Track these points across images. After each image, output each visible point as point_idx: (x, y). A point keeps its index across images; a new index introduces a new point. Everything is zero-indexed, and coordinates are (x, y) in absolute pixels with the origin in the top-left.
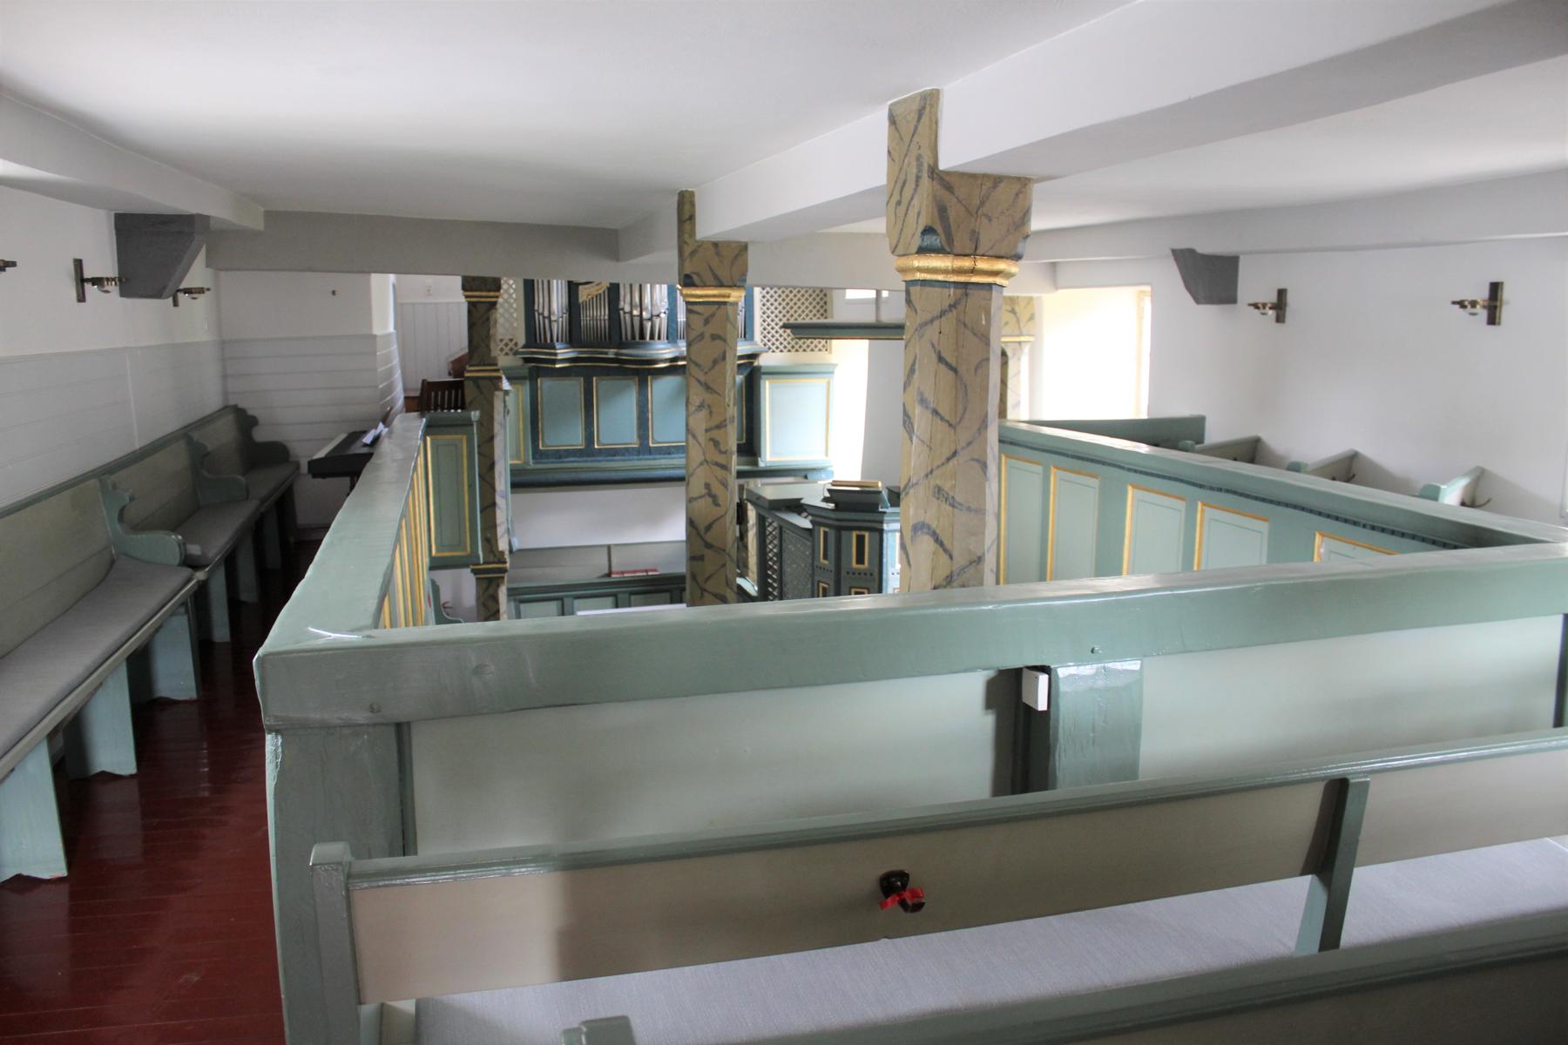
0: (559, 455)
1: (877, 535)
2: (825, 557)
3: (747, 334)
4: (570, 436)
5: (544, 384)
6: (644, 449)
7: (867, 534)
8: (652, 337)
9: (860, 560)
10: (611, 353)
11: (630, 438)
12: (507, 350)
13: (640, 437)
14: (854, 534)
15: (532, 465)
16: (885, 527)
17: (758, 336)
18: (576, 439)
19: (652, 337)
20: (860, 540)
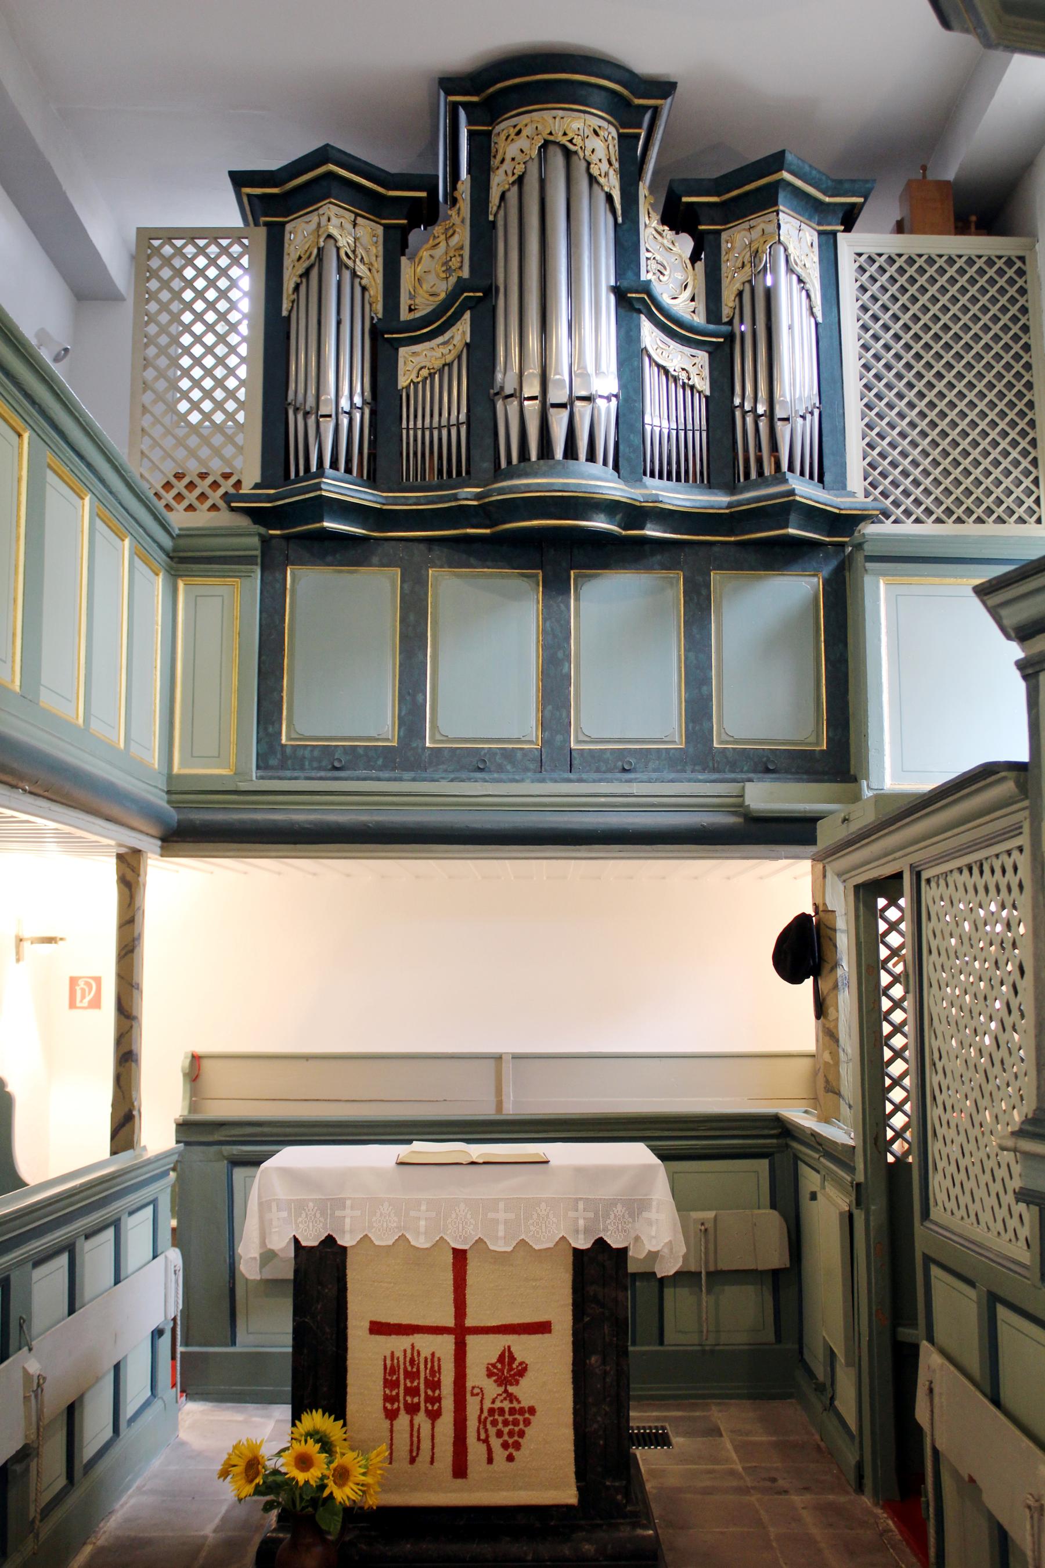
0: (336, 760)
4: (346, 702)
5: (305, 582)
6: (555, 755)
8: (570, 452)
10: (468, 494)
11: (520, 723)
12: (215, 497)
13: (544, 725)
15: (254, 780)
17: (855, 482)
18: (377, 721)
19: (570, 452)
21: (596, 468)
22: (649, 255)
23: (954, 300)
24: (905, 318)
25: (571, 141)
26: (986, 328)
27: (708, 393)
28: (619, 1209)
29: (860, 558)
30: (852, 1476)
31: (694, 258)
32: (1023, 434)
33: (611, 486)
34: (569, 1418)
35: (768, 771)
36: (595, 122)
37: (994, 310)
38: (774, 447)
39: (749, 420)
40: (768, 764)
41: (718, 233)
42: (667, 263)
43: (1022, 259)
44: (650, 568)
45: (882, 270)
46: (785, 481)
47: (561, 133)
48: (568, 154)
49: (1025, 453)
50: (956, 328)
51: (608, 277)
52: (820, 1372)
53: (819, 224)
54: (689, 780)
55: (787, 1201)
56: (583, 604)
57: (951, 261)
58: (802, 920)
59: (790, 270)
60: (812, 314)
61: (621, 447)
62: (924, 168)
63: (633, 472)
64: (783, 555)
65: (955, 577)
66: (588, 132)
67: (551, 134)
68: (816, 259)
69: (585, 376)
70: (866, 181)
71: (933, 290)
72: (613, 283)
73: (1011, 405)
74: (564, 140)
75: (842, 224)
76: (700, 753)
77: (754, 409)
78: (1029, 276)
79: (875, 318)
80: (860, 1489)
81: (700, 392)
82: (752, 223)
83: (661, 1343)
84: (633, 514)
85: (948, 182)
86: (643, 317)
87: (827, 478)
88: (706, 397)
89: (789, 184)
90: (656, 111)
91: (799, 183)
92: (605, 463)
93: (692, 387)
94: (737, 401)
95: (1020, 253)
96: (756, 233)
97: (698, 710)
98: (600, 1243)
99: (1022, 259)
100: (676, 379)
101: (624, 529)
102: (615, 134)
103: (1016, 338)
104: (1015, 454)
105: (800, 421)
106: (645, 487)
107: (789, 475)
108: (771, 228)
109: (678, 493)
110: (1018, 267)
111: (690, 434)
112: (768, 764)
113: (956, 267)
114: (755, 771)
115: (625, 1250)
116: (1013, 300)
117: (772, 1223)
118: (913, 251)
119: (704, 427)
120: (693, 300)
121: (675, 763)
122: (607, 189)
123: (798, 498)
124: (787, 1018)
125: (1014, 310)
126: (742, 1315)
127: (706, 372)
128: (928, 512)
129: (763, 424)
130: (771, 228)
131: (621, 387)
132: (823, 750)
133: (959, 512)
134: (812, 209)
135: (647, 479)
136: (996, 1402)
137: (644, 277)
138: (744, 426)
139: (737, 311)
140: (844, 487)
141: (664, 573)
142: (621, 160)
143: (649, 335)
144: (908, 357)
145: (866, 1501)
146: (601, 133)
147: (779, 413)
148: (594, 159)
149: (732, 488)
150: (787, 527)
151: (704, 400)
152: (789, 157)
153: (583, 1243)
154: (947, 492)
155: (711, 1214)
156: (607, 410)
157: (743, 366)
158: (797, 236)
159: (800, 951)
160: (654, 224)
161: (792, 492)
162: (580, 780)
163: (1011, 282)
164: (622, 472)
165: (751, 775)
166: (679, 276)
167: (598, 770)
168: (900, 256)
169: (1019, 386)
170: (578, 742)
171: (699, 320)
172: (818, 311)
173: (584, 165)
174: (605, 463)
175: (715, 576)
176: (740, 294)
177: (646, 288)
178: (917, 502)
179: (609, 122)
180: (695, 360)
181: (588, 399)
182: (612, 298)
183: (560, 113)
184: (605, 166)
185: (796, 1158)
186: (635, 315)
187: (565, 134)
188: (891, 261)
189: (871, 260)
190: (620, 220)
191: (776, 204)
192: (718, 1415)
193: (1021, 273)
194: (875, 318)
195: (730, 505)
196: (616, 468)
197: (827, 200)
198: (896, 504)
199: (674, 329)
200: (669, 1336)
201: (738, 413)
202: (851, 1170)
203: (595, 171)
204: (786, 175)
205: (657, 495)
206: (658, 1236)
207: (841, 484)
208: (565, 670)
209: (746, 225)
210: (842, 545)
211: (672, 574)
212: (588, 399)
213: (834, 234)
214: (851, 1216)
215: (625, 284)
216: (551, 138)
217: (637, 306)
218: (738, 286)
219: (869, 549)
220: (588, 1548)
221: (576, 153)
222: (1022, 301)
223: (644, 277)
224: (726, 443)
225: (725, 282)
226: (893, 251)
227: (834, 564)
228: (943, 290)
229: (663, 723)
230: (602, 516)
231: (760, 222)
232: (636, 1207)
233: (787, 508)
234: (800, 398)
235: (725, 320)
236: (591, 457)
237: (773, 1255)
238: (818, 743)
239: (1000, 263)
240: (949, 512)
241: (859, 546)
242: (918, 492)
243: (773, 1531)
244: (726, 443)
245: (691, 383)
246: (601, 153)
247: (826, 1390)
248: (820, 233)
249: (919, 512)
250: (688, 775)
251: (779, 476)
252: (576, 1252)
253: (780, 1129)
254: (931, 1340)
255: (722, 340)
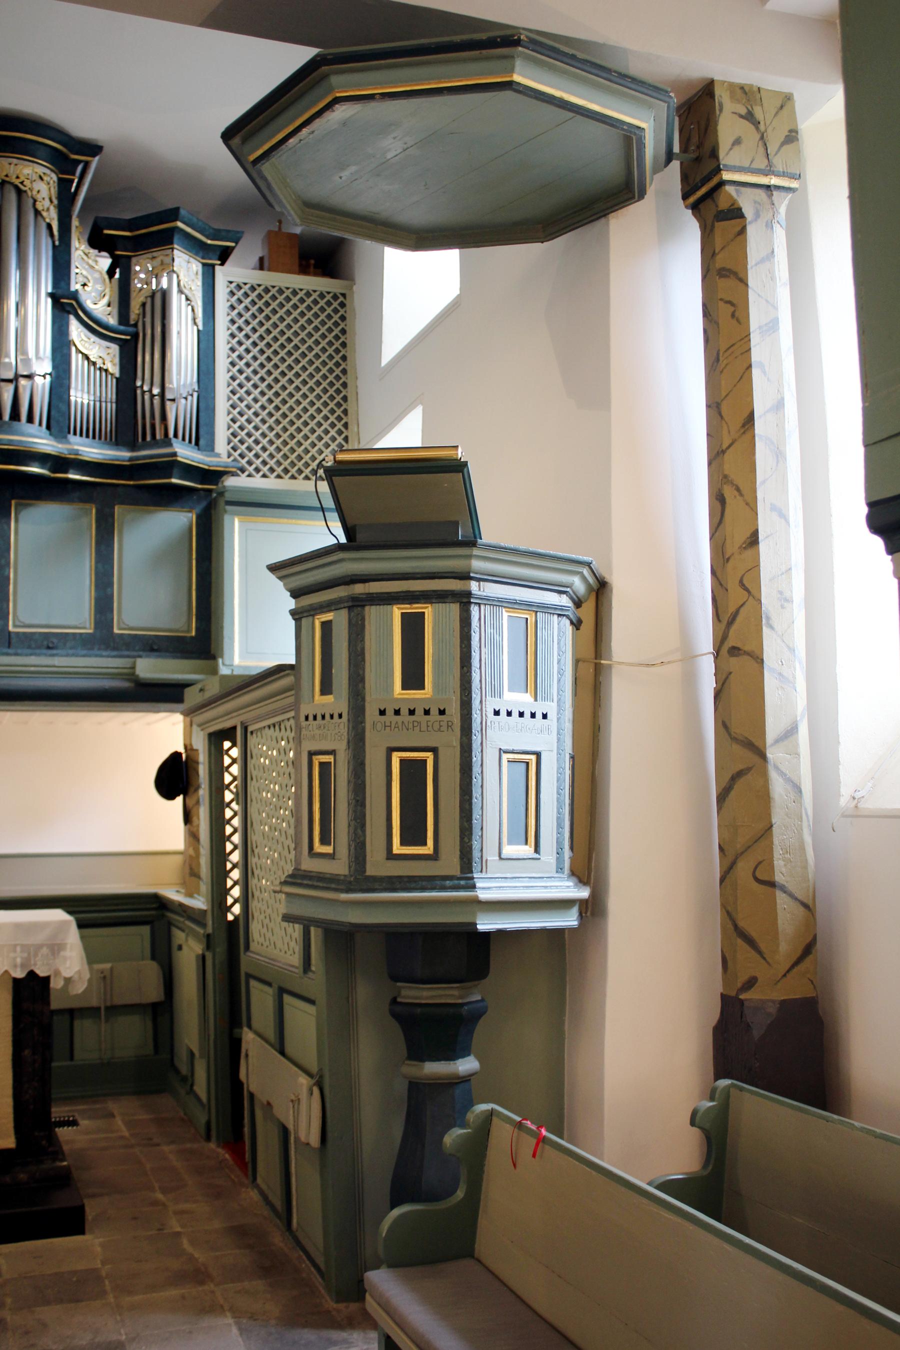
1: (454, 609)
2: (326, 689)
3: (201, 435)
7: (429, 611)
8: (15, 415)
9: (413, 677)
14: (397, 612)
16: (474, 586)
17: (221, 445)
19: (15, 415)
20: (413, 628)
21: (33, 428)
22: (77, 271)
23: (296, 320)
24: (261, 331)
25: (22, 183)
26: (317, 343)
27: (118, 375)
28: (45, 950)
29: (221, 503)
30: (202, 1130)
31: (111, 273)
32: (339, 419)
33: (44, 443)
34: (9, 1091)
35: (152, 650)
36: (40, 170)
37: (323, 330)
38: (164, 418)
39: (147, 397)
40: (153, 645)
41: (130, 257)
42: (90, 270)
43: (344, 295)
44: (70, 501)
45: (246, 295)
46: (169, 444)
47: (14, 177)
48: (20, 192)
49: (340, 432)
50: (296, 341)
51: (47, 286)
52: (184, 1070)
53: (203, 258)
54: (96, 656)
55: (163, 954)
56: (21, 525)
57: (295, 293)
58: (176, 756)
59: (181, 291)
60: (195, 323)
61: (53, 413)
62: (280, 222)
63: (61, 431)
64: (169, 497)
65: (288, 518)
66: (35, 177)
67: (7, 176)
68: (200, 283)
69: (27, 362)
70: (238, 232)
71: (281, 312)
72: (50, 290)
73: (332, 398)
74: (17, 182)
75: (219, 260)
76: (104, 637)
77: (150, 391)
78: (348, 308)
79: (240, 329)
80: (208, 1138)
81: (112, 374)
82: (155, 254)
83: (72, 1058)
84: (59, 463)
85: (296, 235)
86: (72, 317)
87: (202, 442)
88: (117, 378)
89: (182, 230)
90: (87, 165)
91: (189, 230)
92: (40, 424)
93: (106, 371)
94: (139, 383)
95: (343, 292)
96: (157, 262)
97: (104, 605)
98: (32, 974)
99: (344, 295)
100: (94, 364)
101: (54, 471)
102: (55, 177)
103: (337, 351)
104: (333, 432)
105: (183, 401)
106: (69, 443)
107: (174, 440)
108: (167, 260)
109: (94, 448)
110: (341, 301)
111: (104, 405)
112: (153, 645)
113: (298, 297)
114: (144, 650)
115: (47, 979)
116: (336, 324)
117: (152, 970)
118: (269, 284)
119: (114, 400)
120: (109, 305)
121: (85, 643)
122: (48, 220)
123: (179, 459)
124: (163, 826)
125: (336, 331)
126: (130, 1038)
127: (117, 360)
128: (272, 470)
129: (157, 400)
130: (167, 260)
131: (54, 367)
132: (192, 637)
133: (293, 471)
134: (197, 248)
135: (71, 437)
136: (282, 1052)
137: (73, 289)
138: (144, 403)
139: (141, 317)
140: (213, 450)
141: (81, 505)
142: (59, 197)
143: (76, 331)
144: (262, 359)
145: (212, 1145)
146: (45, 178)
147: (169, 395)
148: (39, 197)
149: (133, 447)
150: (170, 477)
151: (114, 380)
152: (183, 212)
153: (20, 974)
154: (286, 457)
155: (108, 966)
156: (42, 384)
157: (145, 359)
158: (186, 268)
159: (173, 778)
160: (83, 247)
161: (175, 454)
162: (16, 654)
163: (336, 311)
164: (53, 430)
165: (141, 653)
166: (99, 287)
167: (29, 647)
168: (259, 285)
169: (338, 385)
170: (15, 626)
171: (112, 321)
172: (200, 321)
173: (31, 201)
174: (40, 424)
175: (117, 509)
176: (144, 305)
177: (75, 296)
178: (265, 463)
179: (52, 170)
180: (110, 351)
181: (30, 377)
182: (50, 300)
183: (15, 161)
184: (47, 203)
185: (170, 924)
186: (66, 315)
187: (18, 177)
188: (253, 289)
189: (239, 287)
190: (57, 243)
191: (172, 243)
192: (112, 1105)
193: (342, 305)
194: (240, 329)
195: (131, 459)
196: (48, 427)
197: (209, 242)
198: (250, 463)
199: (95, 327)
200: (78, 1054)
201: (139, 392)
202: (203, 925)
203: (39, 206)
204: (180, 224)
205: (78, 450)
206: (70, 964)
207: (210, 448)
208: (6, 573)
209: (150, 255)
210: (210, 491)
211: (87, 506)
212: (30, 377)
213: (213, 266)
214: (203, 957)
215: (59, 292)
216: (7, 179)
217: (68, 309)
218: (142, 299)
219: (228, 496)
220: (23, 1176)
221: (25, 191)
222: (342, 325)
223: (73, 289)
224: (131, 413)
225: (133, 295)
226: (255, 282)
227: (204, 504)
228: (289, 313)
229: (78, 616)
230: (37, 464)
231: (160, 255)
232: (56, 948)
233: (172, 465)
234: (184, 385)
235: (132, 322)
236: (30, 420)
237: (153, 993)
238: (189, 631)
239: (328, 297)
240: (286, 471)
241: (221, 494)
242: (265, 456)
243: (148, 1166)
244: (131, 413)
245: (105, 367)
246: (44, 193)
247: (188, 1081)
248: (204, 265)
249: (265, 469)
250: (96, 652)
251: (166, 442)
252: (15, 981)
253: (158, 903)
254: (250, 1027)
255: (128, 337)
